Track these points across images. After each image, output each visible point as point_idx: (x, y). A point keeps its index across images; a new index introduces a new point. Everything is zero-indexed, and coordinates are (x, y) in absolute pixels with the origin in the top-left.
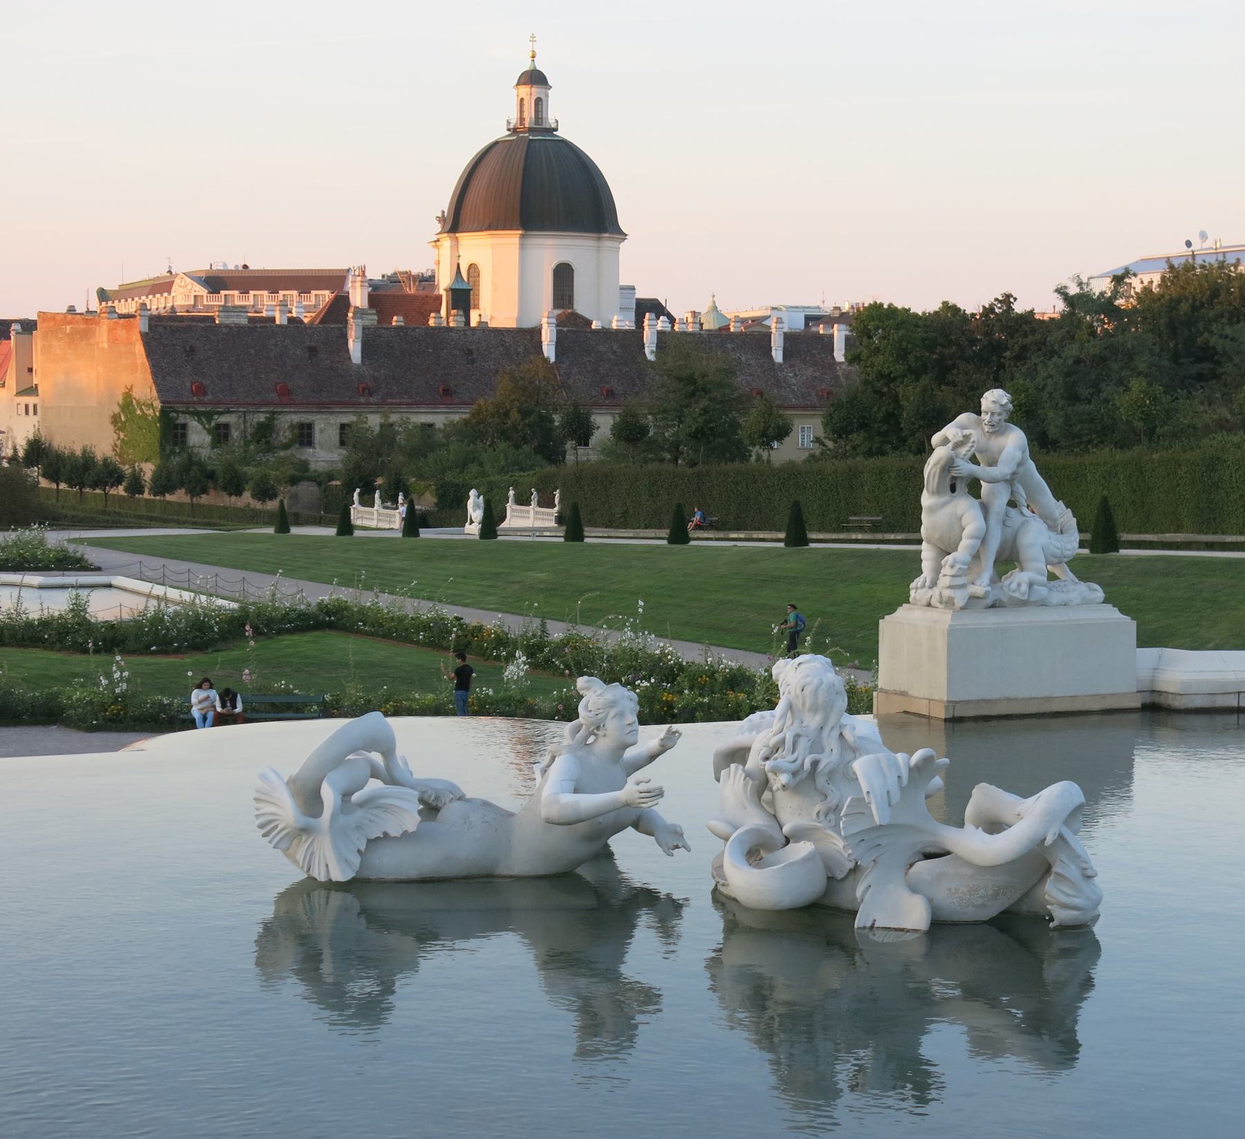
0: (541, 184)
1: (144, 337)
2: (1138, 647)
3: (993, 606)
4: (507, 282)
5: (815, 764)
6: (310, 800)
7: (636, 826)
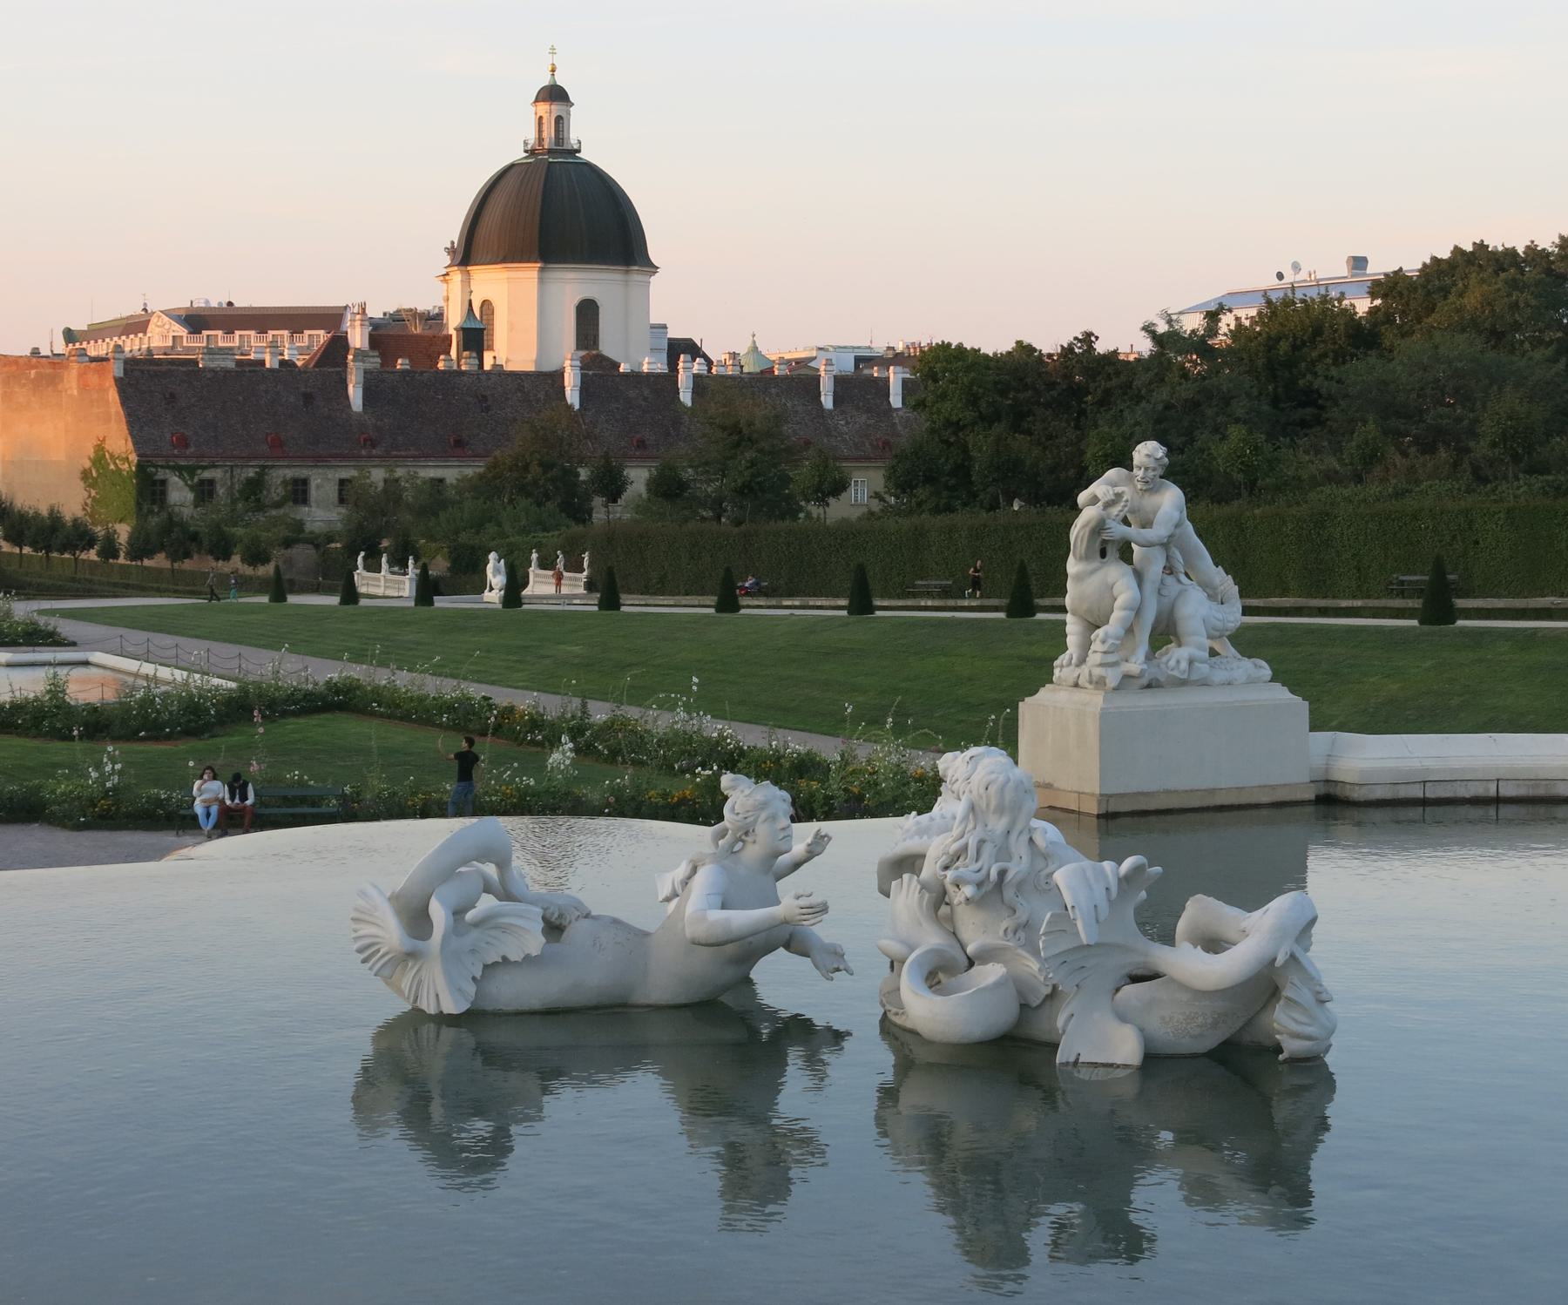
0: (562, 211)
1: (119, 382)
2: (1313, 728)
3: (1149, 686)
4: (523, 319)
5: (1002, 874)
6: (417, 920)
7: (787, 946)
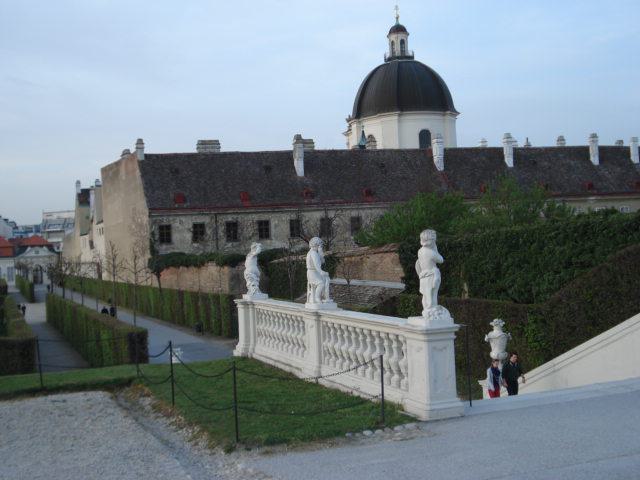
0: (402, 85)
